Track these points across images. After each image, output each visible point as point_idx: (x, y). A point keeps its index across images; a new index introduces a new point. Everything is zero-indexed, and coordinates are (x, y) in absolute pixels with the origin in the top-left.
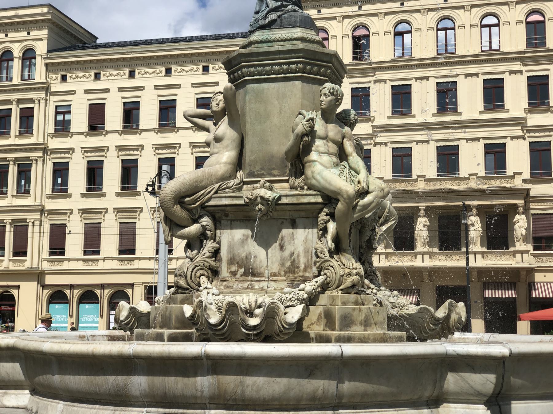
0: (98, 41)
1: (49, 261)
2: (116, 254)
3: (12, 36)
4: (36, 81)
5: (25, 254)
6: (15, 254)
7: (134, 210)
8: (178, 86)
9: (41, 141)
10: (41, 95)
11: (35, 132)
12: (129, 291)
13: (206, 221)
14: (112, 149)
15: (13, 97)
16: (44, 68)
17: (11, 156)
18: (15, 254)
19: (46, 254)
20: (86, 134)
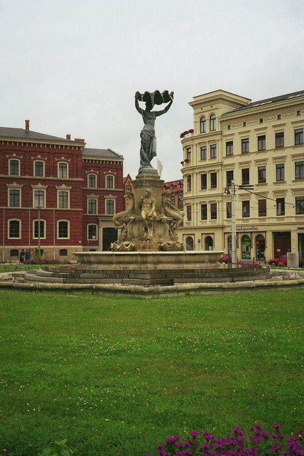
0: (252, 102)
1: (226, 221)
2: (257, 216)
3: (204, 109)
4: (216, 131)
5: (216, 218)
6: (212, 218)
7: (265, 193)
8: (284, 124)
9: (220, 161)
10: (218, 137)
11: (217, 157)
12: (264, 234)
13: (124, 224)
14: (253, 161)
15: (206, 140)
16: (219, 124)
17: (207, 170)
18: (212, 218)
19: (225, 218)
20: (240, 155)
